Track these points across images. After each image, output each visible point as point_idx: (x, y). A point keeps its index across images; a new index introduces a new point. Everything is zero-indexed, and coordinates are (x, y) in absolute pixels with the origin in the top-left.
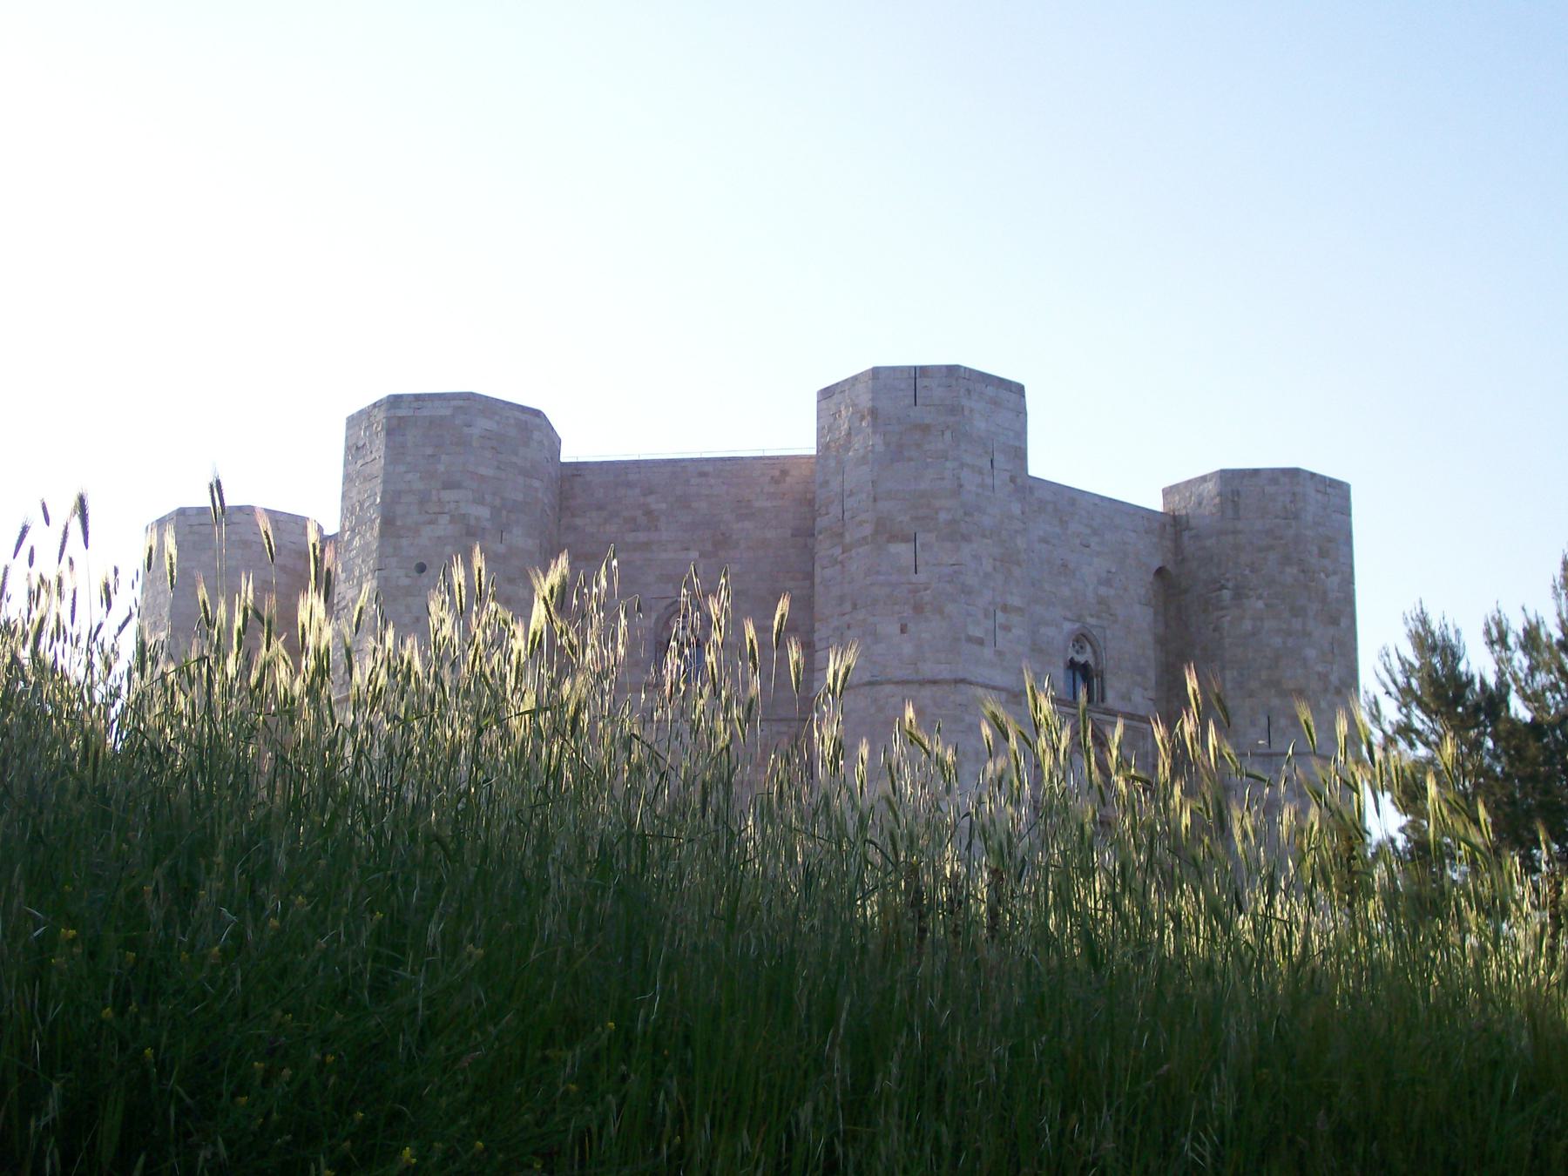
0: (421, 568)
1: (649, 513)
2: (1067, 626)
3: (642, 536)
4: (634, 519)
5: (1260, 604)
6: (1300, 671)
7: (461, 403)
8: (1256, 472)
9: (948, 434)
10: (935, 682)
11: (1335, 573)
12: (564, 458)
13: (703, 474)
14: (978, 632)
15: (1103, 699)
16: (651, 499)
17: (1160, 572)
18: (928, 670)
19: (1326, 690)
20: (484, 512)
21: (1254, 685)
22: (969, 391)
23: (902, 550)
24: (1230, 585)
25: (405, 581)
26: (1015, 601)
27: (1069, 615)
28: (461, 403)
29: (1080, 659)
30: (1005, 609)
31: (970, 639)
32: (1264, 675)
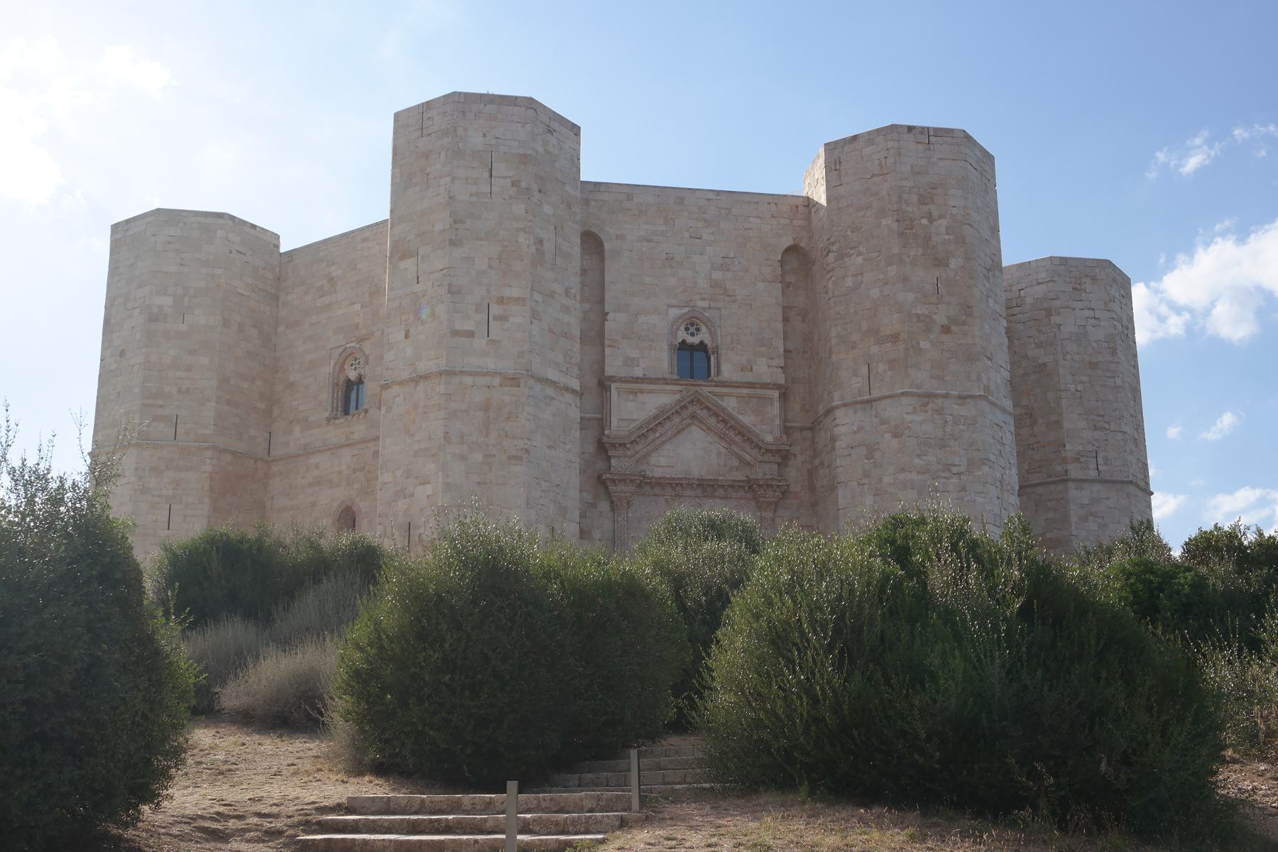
0: (122, 354)
1: (331, 280)
2: (674, 313)
3: (326, 300)
4: (322, 287)
5: (860, 260)
6: (895, 316)
7: (150, 219)
8: (855, 138)
9: (443, 154)
10: (425, 377)
11: (941, 217)
12: (282, 250)
13: (365, 240)
14: (468, 326)
15: (718, 373)
16: (333, 268)
17: (792, 250)
18: (424, 366)
19: (928, 330)
20: (166, 301)
21: (855, 337)
22: (464, 113)
23: (409, 264)
24: (834, 248)
25: (114, 366)
26: (515, 292)
27: (674, 302)
28: (150, 219)
29: (694, 340)
30: (501, 301)
31: (456, 333)
32: (864, 327)
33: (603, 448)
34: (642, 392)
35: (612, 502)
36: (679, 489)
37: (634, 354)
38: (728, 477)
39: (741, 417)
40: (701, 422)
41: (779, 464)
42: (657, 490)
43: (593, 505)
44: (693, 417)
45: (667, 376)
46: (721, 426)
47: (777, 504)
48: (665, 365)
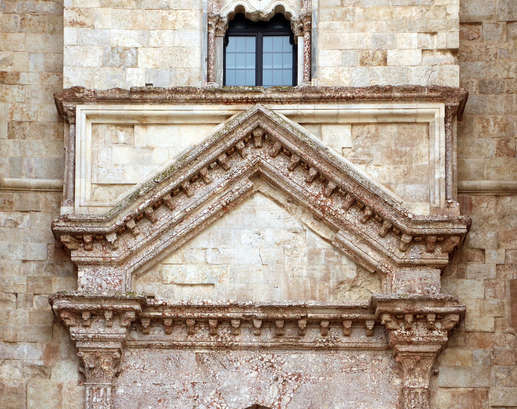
33: (66, 246)
34: (144, 121)
35: (82, 364)
36: (224, 332)
37: (128, 39)
38: (331, 301)
39: (360, 169)
40: (275, 186)
41: (444, 271)
42: (179, 336)
43: (43, 371)
44: (257, 175)
45: (200, 84)
46: (314, 189)
47: (438, 356)
48: (195, 62)
